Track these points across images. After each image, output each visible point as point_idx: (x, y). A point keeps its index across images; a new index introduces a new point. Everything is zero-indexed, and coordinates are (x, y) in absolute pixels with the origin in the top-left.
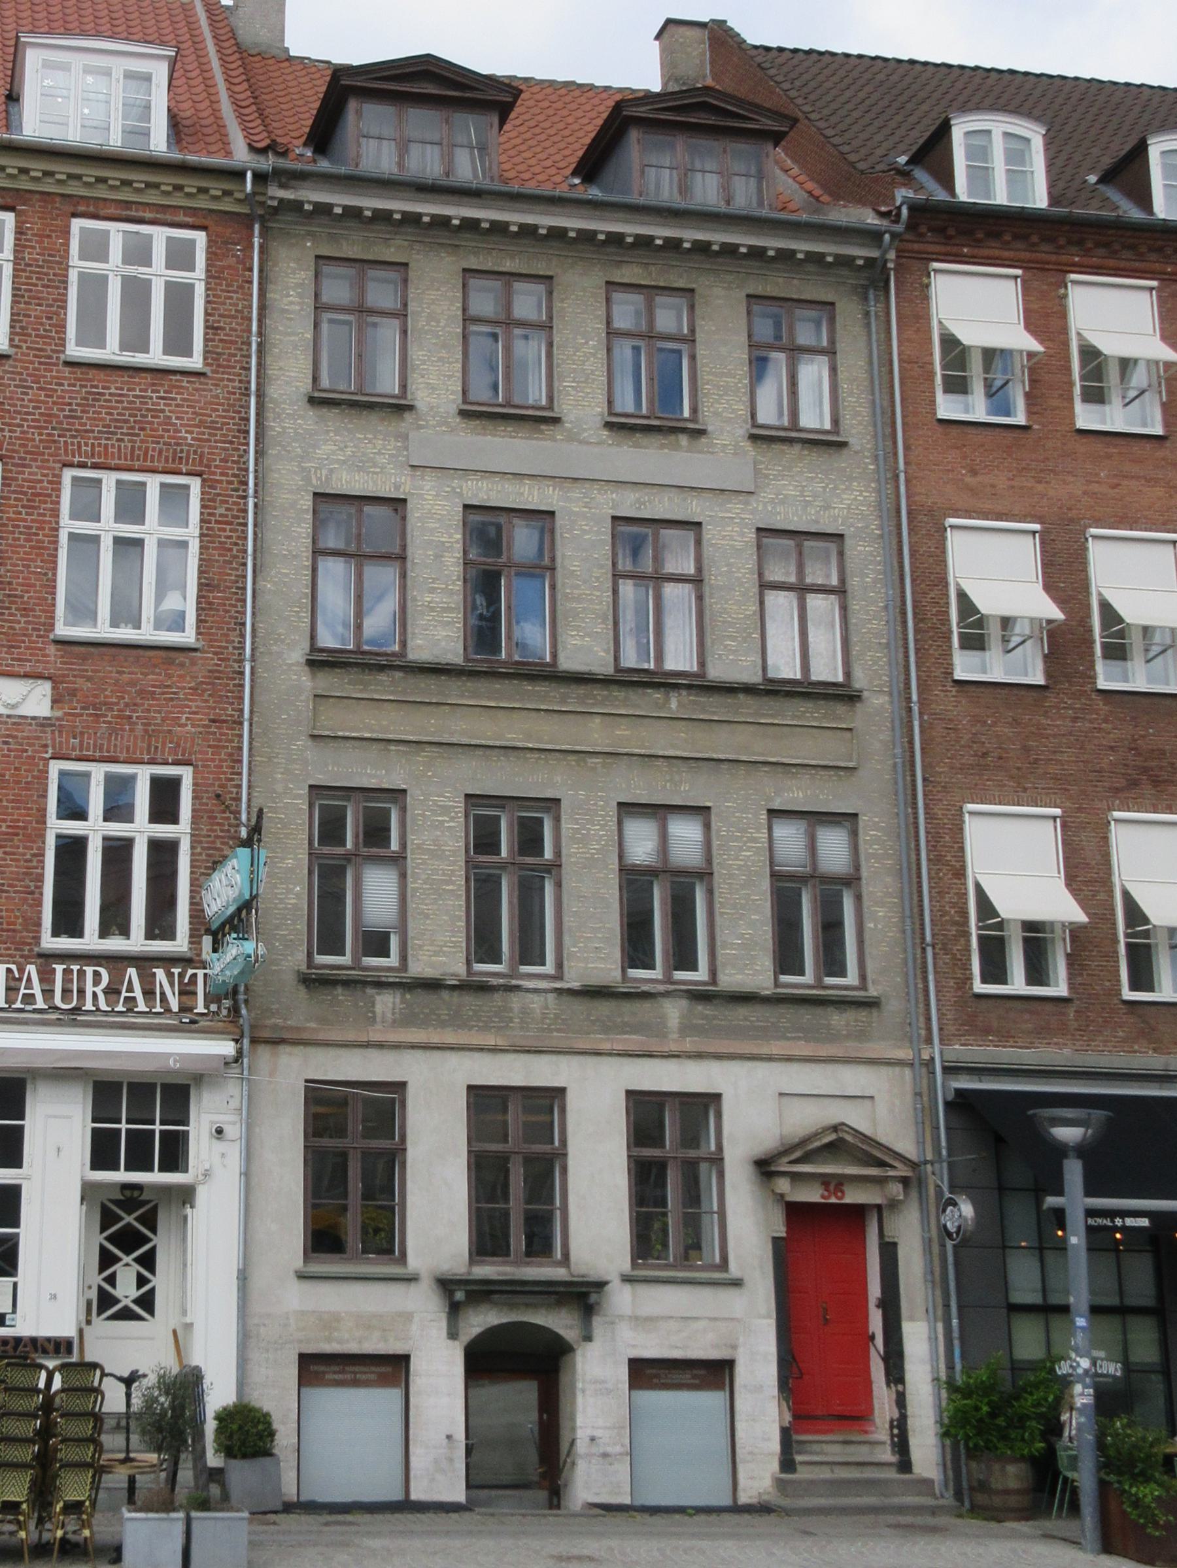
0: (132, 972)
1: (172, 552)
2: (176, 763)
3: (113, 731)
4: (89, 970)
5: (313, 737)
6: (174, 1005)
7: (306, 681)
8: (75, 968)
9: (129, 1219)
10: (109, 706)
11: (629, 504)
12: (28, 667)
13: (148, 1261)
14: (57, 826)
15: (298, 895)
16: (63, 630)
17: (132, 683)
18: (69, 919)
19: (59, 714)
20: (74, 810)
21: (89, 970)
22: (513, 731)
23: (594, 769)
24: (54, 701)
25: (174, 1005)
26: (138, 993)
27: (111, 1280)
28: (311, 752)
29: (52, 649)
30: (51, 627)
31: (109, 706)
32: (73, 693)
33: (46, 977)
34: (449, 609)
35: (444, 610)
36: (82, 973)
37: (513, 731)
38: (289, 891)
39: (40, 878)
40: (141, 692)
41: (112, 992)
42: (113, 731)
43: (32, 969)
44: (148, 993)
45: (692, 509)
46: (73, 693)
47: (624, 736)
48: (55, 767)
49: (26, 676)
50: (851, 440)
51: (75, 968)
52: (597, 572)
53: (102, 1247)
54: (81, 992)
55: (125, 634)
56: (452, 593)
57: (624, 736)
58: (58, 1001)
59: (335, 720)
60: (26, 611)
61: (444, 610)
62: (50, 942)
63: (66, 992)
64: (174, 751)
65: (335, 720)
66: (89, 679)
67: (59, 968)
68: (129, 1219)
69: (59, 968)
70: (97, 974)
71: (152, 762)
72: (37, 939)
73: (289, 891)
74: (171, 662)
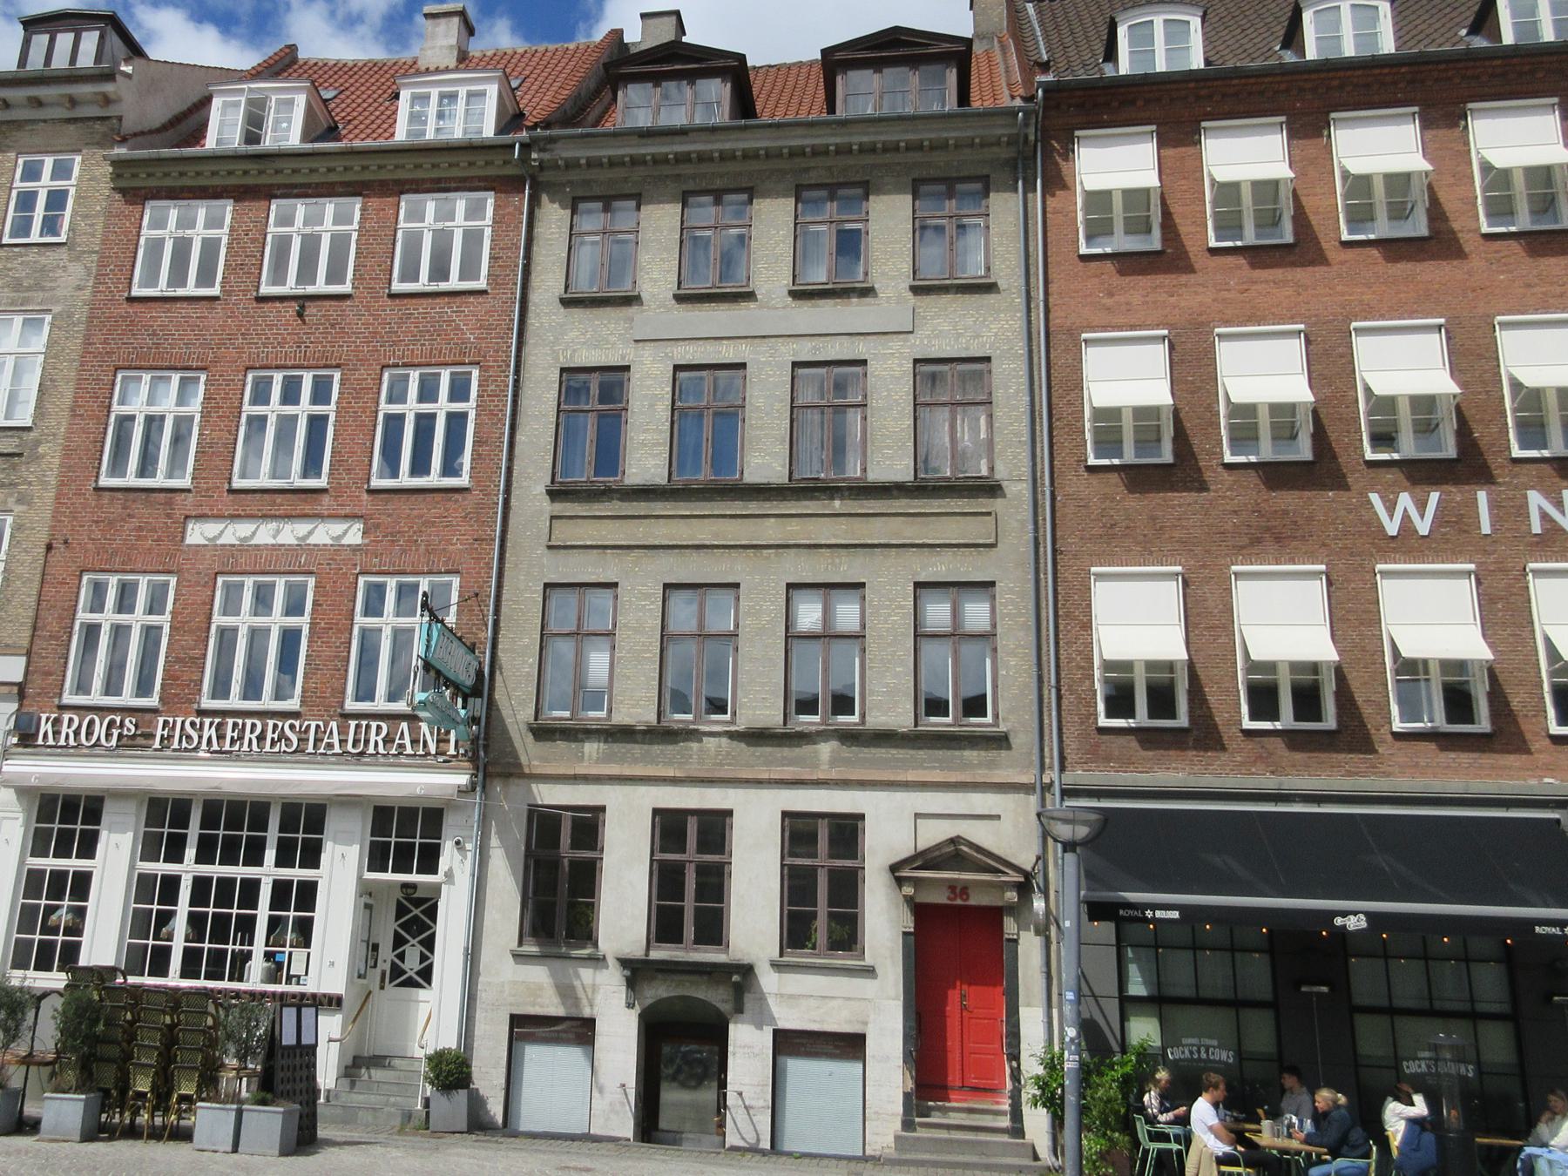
0: (404, 725)
2: (448, 572)
4: (374, 725)
5: (550, 547)
6: (432, 748)
7: (547, 507)
8: (364, 723)
9: (416, 912)
11: (806, 351)
12: (347, 510)
13: (429, 944)
15: (531, 666)
21: (374, 725)
22: (703, 532)
23: (768, 558)
25: (432, 748)
26: (407, 741)
27: (401, 957)
28: (548, 558)
33: (343, 730)
34: (658, 444)
35: (655, 445)
36: (368, 727)
37: (703, 532)
38: (525, 662)
41: (388, 741)
43: (334, 725)
44: (414, 742)
45: (859, 349)
46: (377, 526)
47: (795, 531)
49: (346, 516)
50: (1002, 284)
52: (777, 406)
53: (396, 932)
54: (367, 742)
56: (661, 432)
57: (795, 531)
58: (349, 747)
59: (569, 533)
61: (655, 445)
62: (351, 705)
63: (356, 743)
64: (446, 563)
65: (569, 533)
67: (353, 724)
68: (416, 912)
70: (379, 727)
73: (525, 662)
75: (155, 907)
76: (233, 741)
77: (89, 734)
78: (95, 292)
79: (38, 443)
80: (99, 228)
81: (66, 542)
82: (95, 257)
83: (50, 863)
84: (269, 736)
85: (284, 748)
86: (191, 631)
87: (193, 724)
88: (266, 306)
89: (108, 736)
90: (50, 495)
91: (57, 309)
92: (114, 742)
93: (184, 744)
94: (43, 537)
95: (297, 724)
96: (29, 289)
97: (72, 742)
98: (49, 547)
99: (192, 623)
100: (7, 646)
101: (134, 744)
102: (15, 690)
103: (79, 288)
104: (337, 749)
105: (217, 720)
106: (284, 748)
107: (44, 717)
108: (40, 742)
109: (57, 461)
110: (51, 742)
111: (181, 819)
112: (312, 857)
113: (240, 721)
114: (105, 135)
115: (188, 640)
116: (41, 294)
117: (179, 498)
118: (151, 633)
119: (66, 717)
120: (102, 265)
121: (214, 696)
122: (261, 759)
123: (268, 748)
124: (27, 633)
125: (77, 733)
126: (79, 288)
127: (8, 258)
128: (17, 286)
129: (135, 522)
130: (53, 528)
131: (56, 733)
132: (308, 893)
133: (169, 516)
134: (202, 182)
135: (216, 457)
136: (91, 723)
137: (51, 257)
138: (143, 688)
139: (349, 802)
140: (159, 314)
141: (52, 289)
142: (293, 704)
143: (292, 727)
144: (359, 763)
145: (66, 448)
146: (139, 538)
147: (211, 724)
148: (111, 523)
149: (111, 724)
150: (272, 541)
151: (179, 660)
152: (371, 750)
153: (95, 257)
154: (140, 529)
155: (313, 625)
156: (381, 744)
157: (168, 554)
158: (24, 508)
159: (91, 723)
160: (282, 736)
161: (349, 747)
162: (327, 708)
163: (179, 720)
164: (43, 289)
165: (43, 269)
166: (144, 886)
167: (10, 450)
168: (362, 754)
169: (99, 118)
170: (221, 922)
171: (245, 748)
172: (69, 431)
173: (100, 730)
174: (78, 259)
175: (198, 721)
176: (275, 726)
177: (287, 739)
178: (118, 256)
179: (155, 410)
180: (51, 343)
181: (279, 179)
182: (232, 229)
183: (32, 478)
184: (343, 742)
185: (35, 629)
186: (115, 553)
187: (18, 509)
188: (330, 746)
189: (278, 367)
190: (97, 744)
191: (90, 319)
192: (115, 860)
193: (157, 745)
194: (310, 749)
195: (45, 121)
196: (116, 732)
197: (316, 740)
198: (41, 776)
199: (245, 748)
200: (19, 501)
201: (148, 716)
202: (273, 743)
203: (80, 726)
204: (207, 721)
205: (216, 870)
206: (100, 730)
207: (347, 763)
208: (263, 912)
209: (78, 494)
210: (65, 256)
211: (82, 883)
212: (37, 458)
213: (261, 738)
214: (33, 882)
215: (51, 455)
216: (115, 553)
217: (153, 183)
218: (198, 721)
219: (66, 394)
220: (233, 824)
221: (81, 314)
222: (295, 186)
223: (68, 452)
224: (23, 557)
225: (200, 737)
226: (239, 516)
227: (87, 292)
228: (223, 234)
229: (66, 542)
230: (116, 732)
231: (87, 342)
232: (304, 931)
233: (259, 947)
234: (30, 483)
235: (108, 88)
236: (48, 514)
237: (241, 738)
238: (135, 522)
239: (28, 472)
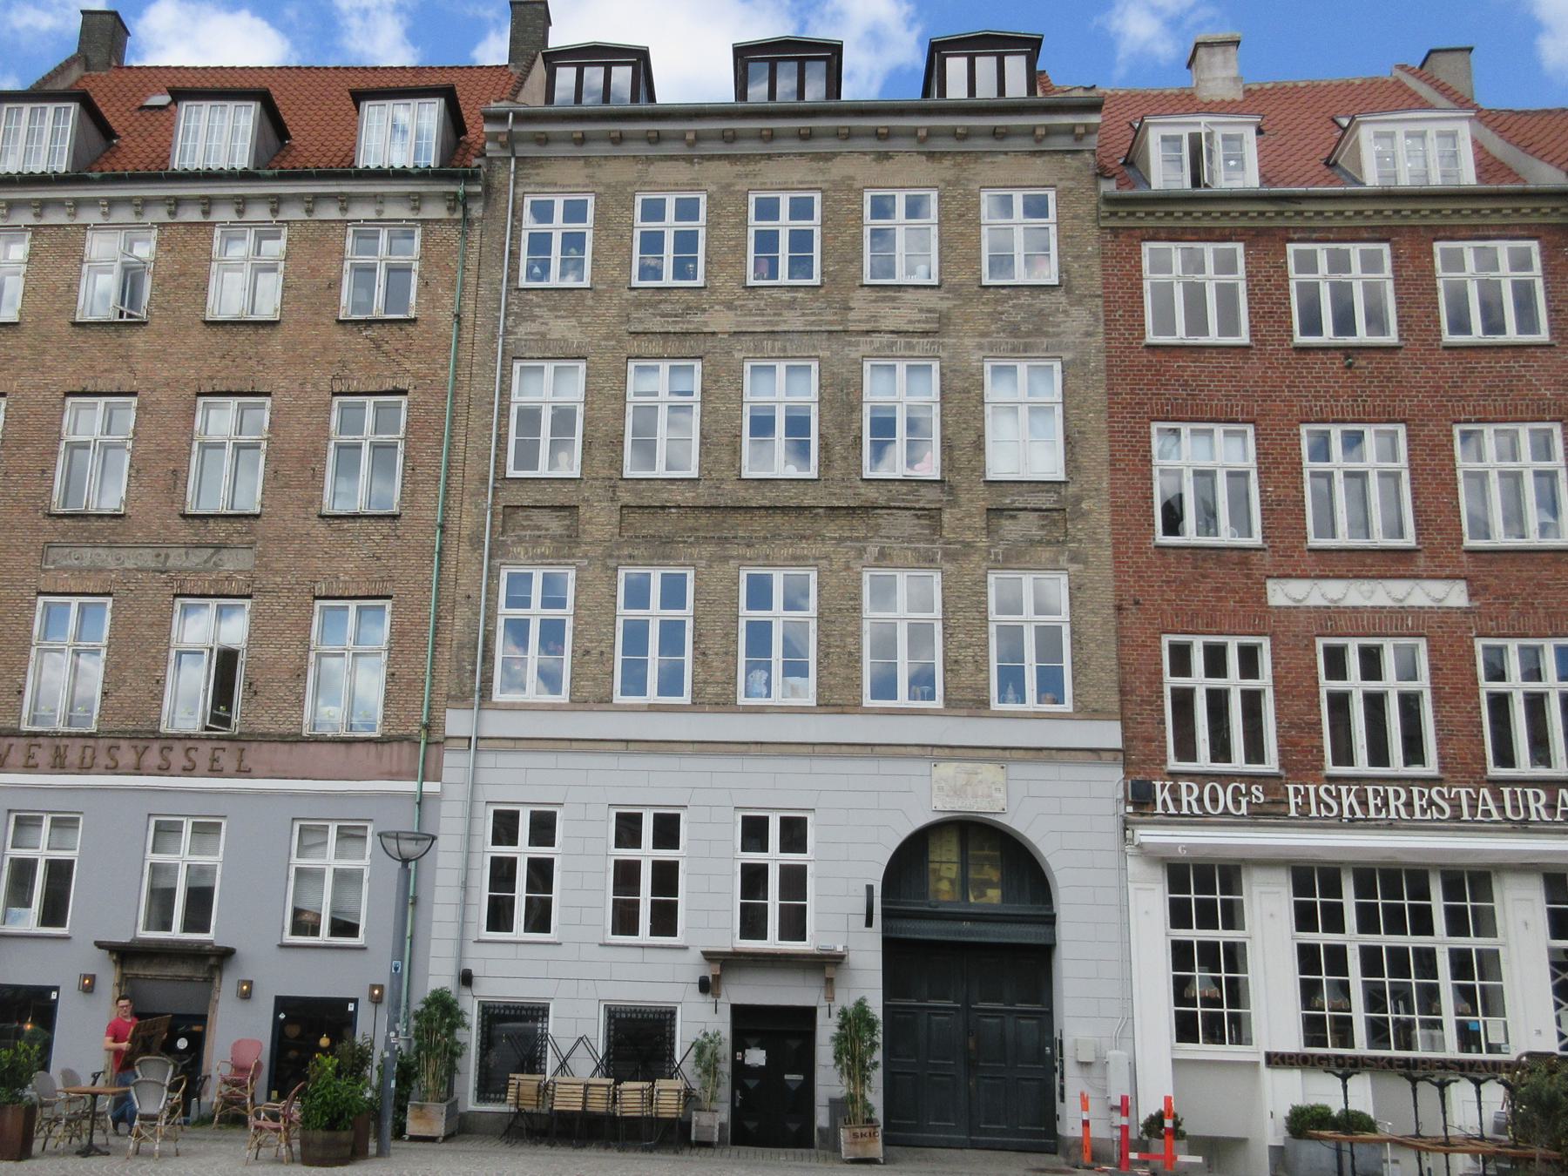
1: (1546, 481)
3: (1522, 614)
4: (1530, 792)
8: (1519, 790)
10: (1515, 596)
14: (1486, 687)
16: (1469, 543)
17: (1530, 579)
18: (1505, 756)
19: (1477, 604)
20: (1498, 674)
21: (1530, 792)
24: (1472, 595)
29: (1464, 557)
30: (1460, 541)
31: (1515, 596)
32: (1486, 588)
33: (1498, 797)
36: (1525, 794)
39: (1480, 725)
40: (1540, 585)
42: (1522, 614)
43: (1485, 791)
48: (1479, 644)
49: (1447, 578)
51: (1519, 790)
54: (1527, 808)
55: (1515, 543)
60: (1440, 530)
62: (1494, 771)
63: (1515, 808)
66: (1497, 577)
67: (1506, 791)
69: (1506, 791)
70: (1537, 797)
71: (1555, 635)
72: (1485, 769)
74: (1558, 561)
75: (1413, 980)
76: (1378, 810)
77: (1214, 800)
78: (1108, 340)
79: (1078, 500)
80: (1097, 269)
81: (1137, 603)
82: (1099, 301)
83: (1195, 935)
84: (1417, 803)
85: (1436, 815)
86: (1300, 696)
87: (1328, 791)
88: (1309, 358)
89: (1237, 803)
90: (1109, 552)
91: (1067, 356)
92: (1244, 810)
93: (1324, 813)
94: (1108, 597)
95: (1445, 790)
96: (1029, 334)
97: (1196, 810)
98: (1119, 608)
99: (1294, 689)
100: (1095, 711)
101: (1270, 812)
102: (1121, 756)
103: (1088, 334)
104: (1496, 816)
105: (1354, 788)
106: (1436, 815)
107: (1158, 784)
108: (1159, 809)
109: (1106, 518)
110: (1172, 810)
111: (1332, 885)
112: (1486, 925)
113: (1381, 789)
114: (1079, 170)
115: (1300, 705)
116: (1045, 340)
117: (1255, 558)
118: (1252, 701)
119: (1183, 785)
120: (1108, 313)
121: (1336, 762)
122: (1414, 827)
123: (1418, 815)
124: (1116, 698)
125: (1200, 800)
126: (1088, 334)
127: (997, 301)
128: (1014, 330)
129: (1210, 583)
130: (1118, 588)
131: (1177, 801)
132: (1490, 962)
133: (1248, 576)
134: (1206, 223)
135: (1283, 512)
136: (1213, 789)
137: (1044, 301)
138: (1255, 752)
139: (1522, 868)
140: (1190, 366)
141: (1058, 335)
142: (1431, 768)
143: (1439, 792)
144: (1527, 831)
145: (1114, 505)
146: (1220, 599)
147: (1349, 791)
148: (1184, 583)
149: (1236, 790)
150: (1369, 603)
151: (1292, 725)
152: (1534, 817)
153: (1099, 301)
154: (1217, 590)
155: (1436, 691)
156: (1543, 811)
157: (1259, 616)
158: (1081, 566)
159: (1213, 789)
160: (1431, 803)
161: (1509, 813)
162: (1472, 774)
163: (1311, 788)
164: (1046, 334)
165: (1041, 313)
166: (1308, 957)
167: (1048, 506)
168: (1526, 821)
169: (1069, 152)
170: (1401, 995)
171: (1393, 815)
172: (1112, 484)
173: (1225, 798)
174: (1079, 302)
175: (1332, 788)
176: (1422, 794)
177: (1437, 806)
178: (1122, 299)
179: (1204, 464)
180: (1066, 392)
181: (1298, 222)
182: (1250, 276)
183: (1081, 535)
184: (1502, 809)
185: (1122, 692)
186: (1196, 614)
187: (1074, 567)
188: (1487, 813)
189: (1335, 421)
190: (1226, 812)
191: (1109, 367)
192: (1268, 928)
193: (1293, 813)
194: (1466, 816)
195: (1006, 153)
196: (1244, 801)
197: (1470, 806)
198: (1189, 847)
199: (1393, 815)
200: (1073, 560)
201: (1273, 783)
202: (1424, 811)
203: (1201, 792)
204: (1344, 789)
205: (1384, 940)
206: (1225, 798)
207: (1514, 830)
208: (1445, 982)
209: (1139, 552)
210: (1063, 300)
211: (1235, 954)
212: (1084, 515)
213: (1409, 805)
214: (1181, 954)
215: (1098, 511)
216: (1196, 614)
217: (1151, 222)
218: (1332, 788)
219: (1099, 450)
220: (1394, 890)
221: (1097, 362)
222: (1314, 229)
223: (1116, 509)
224: (1090, 618)
225: (1340, 805)
226: (1327, 577)
227: (1100, 338)
228: (1239, 279)
229: (1137, 603)
230: (1244, 801)
231: (1111, 392)
232: (1493, 1004)
233: (1449, 1017)
234: (1080, 541)
235: (1095, 119)
236: (1109, 573)
237: (1386, 804)
238: (1210, 583)
239: (1077, 528)
